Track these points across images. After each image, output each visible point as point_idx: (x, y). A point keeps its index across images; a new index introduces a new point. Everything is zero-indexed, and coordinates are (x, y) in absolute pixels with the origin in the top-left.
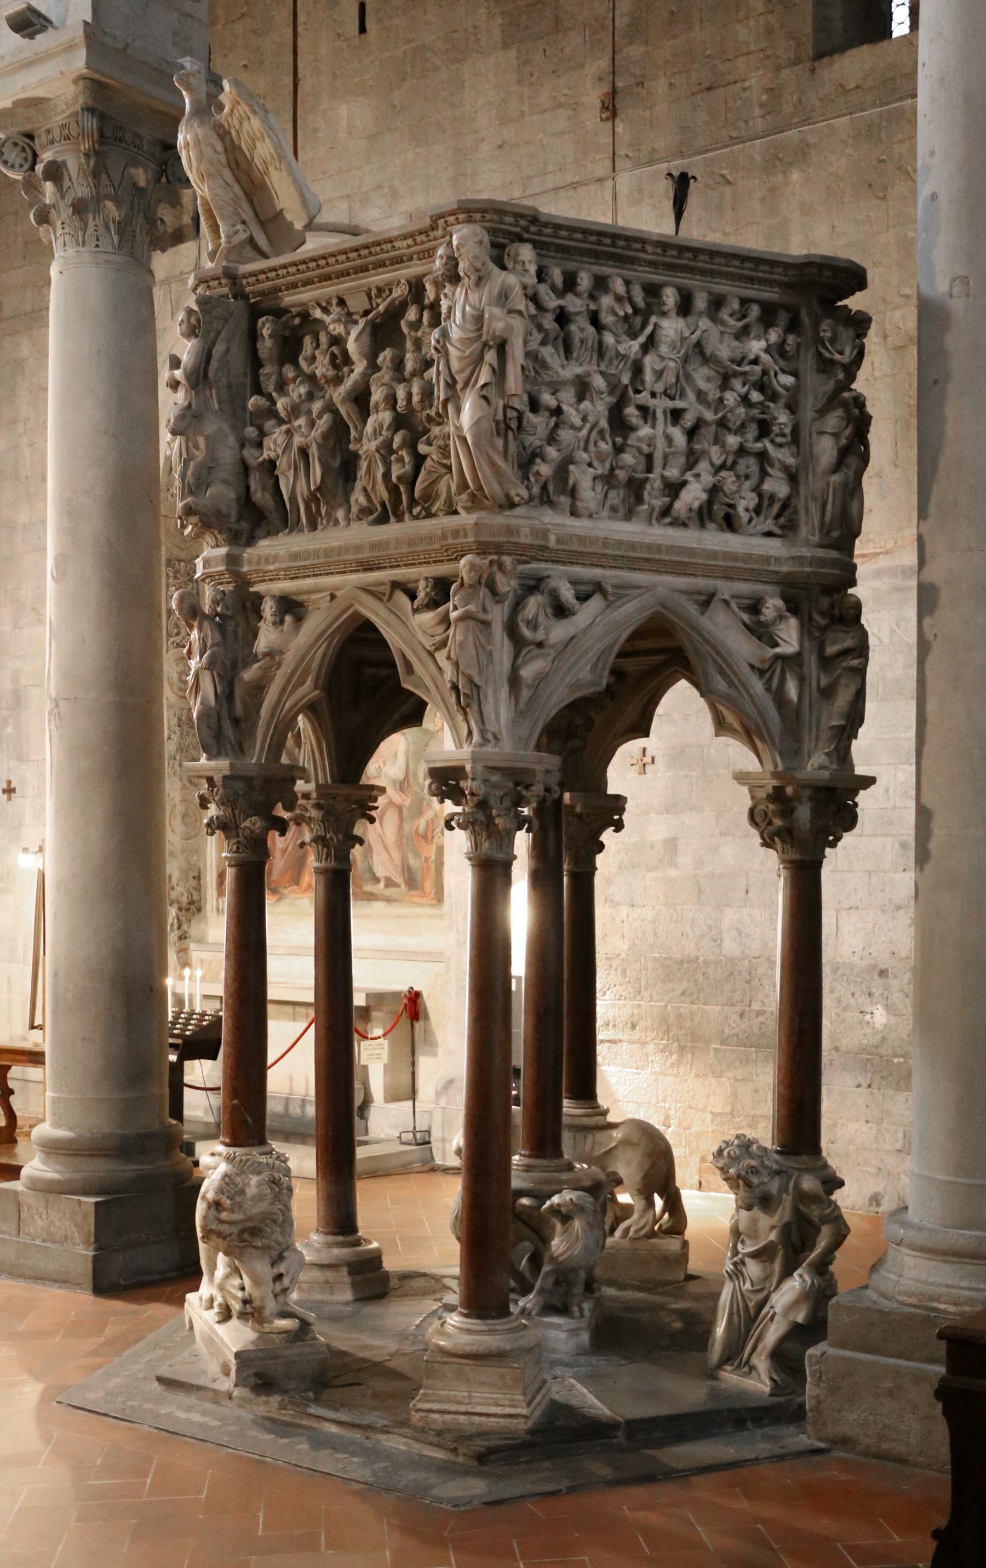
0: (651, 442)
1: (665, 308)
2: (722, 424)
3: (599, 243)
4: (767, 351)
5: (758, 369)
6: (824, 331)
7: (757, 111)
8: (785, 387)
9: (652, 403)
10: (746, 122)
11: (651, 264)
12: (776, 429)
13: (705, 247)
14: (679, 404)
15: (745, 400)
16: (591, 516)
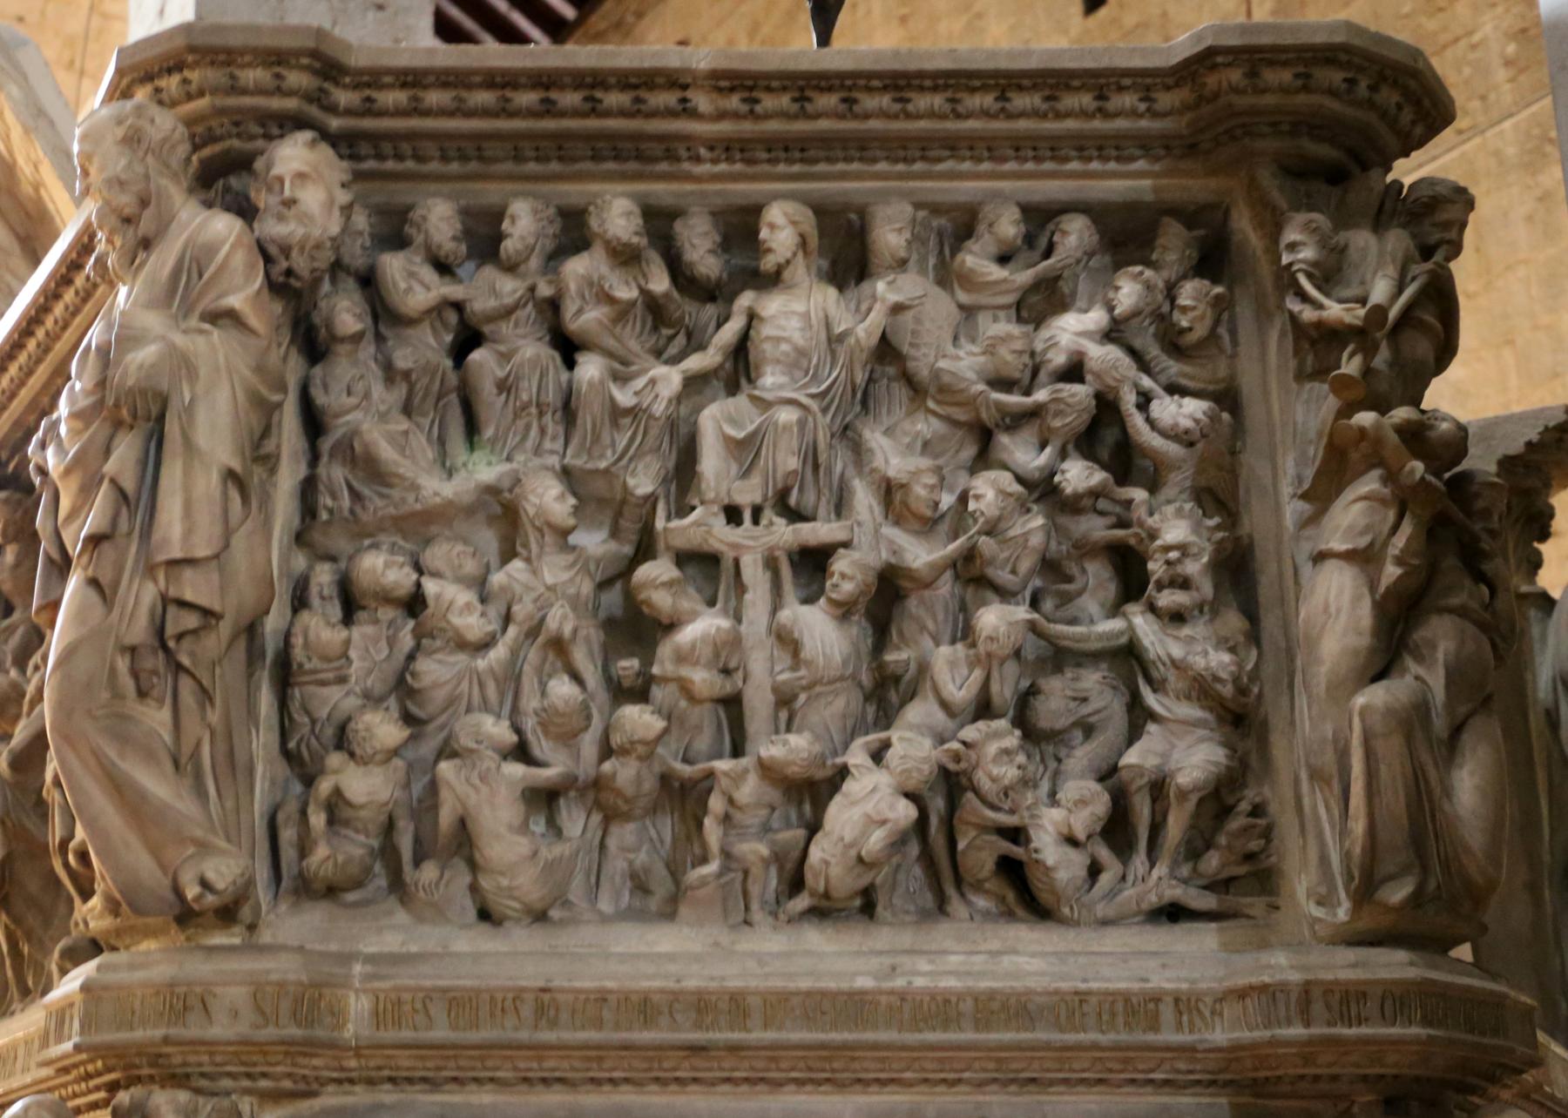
0: (726, 656)
1: (768, 263)
2: (972, 575)
3: (548, 109)
4: (1113, 334)
5: (1080, 393)
6: (1292, 247)
7: (1501, 74)
8: (1184, 438)
9: (721, 535)
10: (1483, 98)
11: (728, 148)
12: (1156, 567)
13: (867, 65)
14: (821, 531)
15: (1043, 489)
16: (540, 917)
